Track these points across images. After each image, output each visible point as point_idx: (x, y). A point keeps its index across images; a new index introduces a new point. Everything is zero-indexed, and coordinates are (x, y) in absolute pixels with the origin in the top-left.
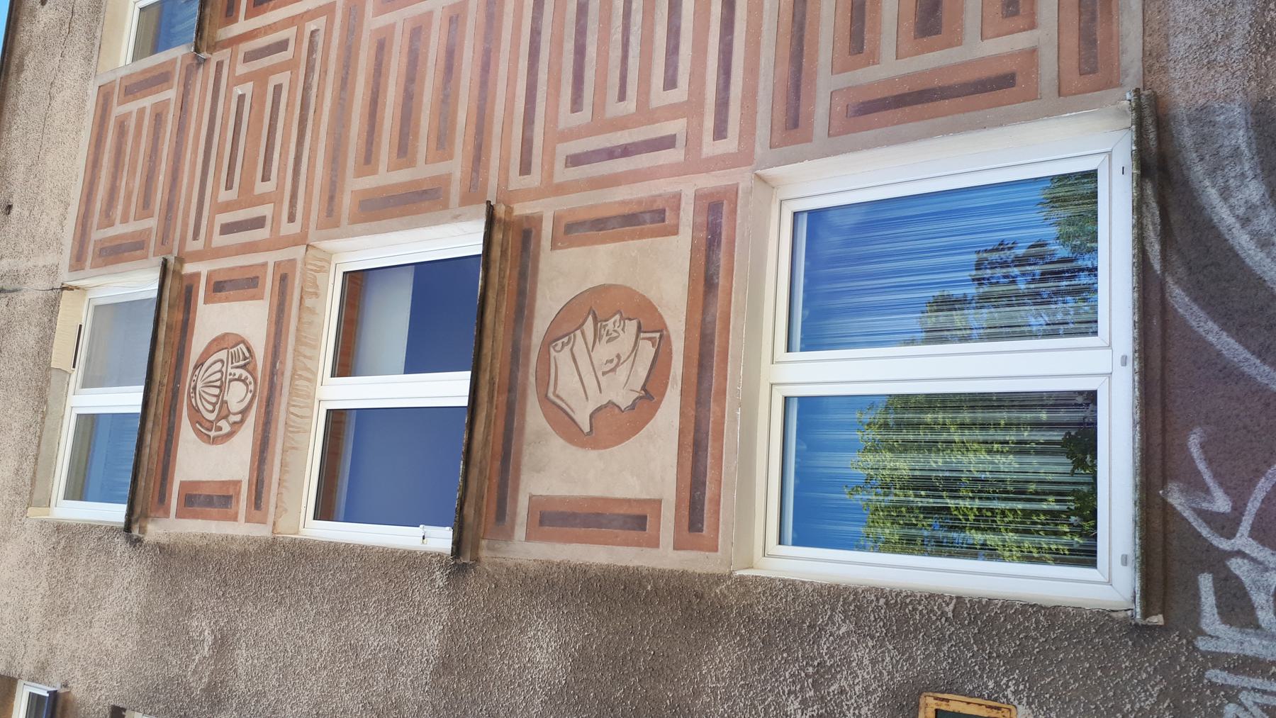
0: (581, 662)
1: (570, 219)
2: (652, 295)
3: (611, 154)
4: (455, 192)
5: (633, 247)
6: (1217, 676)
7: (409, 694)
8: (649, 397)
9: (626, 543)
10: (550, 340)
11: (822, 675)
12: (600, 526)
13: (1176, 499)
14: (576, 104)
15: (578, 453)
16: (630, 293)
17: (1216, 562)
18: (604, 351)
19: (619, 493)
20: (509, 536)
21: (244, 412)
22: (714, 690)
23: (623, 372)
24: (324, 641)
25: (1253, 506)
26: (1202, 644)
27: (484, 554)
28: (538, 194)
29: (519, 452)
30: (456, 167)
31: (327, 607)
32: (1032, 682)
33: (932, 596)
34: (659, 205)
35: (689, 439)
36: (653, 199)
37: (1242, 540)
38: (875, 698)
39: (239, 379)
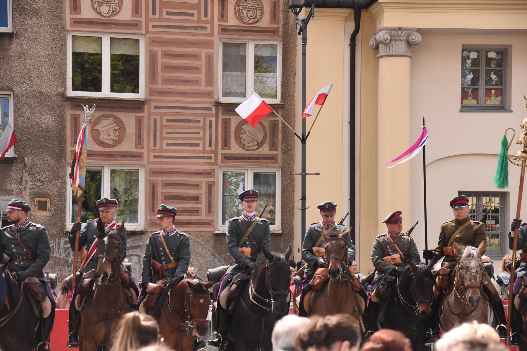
0: (47, 131)
1: (142, 121)
2: (123, 143)
3: (155, 131)
4: (153, 86)
5: (134, 138)
6: (57, 240)
7: (34, 83)
8: (101, 143)
9: (71, 139)
10: (115, 117)
12: (74, 133)
14: (168, 121)
16: (123, 138)
18: (111, 132)
20: (72, 109)
21: (100, 13)
22: (45, 160)
23: (107, 137)
24: (42, 53)
26: (61, 238)
27: (67, 103)
28: (149, 111)
30: (159, 86)
31: (51, 53)
32: (53, 216)
33: (66, 200)
34: (142, 143)
35: (92, 153)
36: (143, 142)
38: (48, 191)
39: (109, 10)
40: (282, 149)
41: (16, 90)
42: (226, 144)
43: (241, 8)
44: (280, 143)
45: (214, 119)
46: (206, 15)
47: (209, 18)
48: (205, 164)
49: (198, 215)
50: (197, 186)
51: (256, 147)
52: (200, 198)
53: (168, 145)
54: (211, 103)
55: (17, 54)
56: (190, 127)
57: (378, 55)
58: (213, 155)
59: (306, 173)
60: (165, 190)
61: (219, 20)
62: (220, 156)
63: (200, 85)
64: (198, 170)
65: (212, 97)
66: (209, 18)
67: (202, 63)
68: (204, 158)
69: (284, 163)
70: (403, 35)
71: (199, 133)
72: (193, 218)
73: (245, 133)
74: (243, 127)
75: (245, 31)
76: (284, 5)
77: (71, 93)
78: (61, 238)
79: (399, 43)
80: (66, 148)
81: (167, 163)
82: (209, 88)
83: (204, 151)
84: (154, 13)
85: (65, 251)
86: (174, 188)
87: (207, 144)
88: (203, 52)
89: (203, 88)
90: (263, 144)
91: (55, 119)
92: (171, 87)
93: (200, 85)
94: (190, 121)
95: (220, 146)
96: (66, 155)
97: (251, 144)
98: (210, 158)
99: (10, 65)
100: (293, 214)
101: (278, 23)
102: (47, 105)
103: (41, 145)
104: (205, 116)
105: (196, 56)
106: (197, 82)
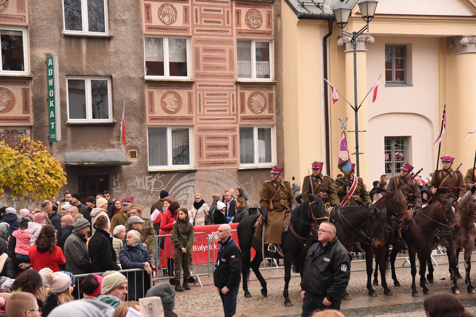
0: (134, 103)
1: (192, 95)
2: (180, 111)
3: (200, 102)
4: (198, 71)
6: (143, 177)
7: (125, 71)
8: (167, 111)
10: (175, 93)
11: (137, 138)
13: (158, 174)
14: (207, 95)
15: (160, 100)
16: (181, 107)
17: (153, 177)
18: (173, 103)
19: (155, 107)
20: (148, 88)
21: (163, 22)
22: (133, 124)
23: (171, 107)
24: (129, 50)
25: (158, 180)
26: (146, 176)
28: (196, 88)
29: (159, 89)
30: (201, 71)
32: (140, 161)
34: (192, 111)
35: (162, 118)
36: (193, 110)
37: (155, 179)
39: (169, 20)
40: (276, 112)
41: (114, 76)
42: (243, 110)
43: (249, 17)
44: (274, 108)
45: (235, 93)
46: (228, 23)
47: (230, 25)
48: (230, 123)
49: (227, 158)
50: (226, 138)
51: (261, 111)
52: (228, 146)
53: (208, 111)
54: (233, 82)
55: (114, 51)
56: (221, 99)
57: (345, 51)
58: (235, 117)
59: (358, 130)
60: (207, 142)
61: (236, 26)
62: (239, 118)
63: (226, 70)
64: (227, 127)
65: (234, 78)
66: (230, 25)
67: (227, 55)
68: (230, 119)
69: (277, 121)
70: (364, 38)
71: (226, 103)
72: (225, 160)
73: (254, 102)
74: (252, 98)
75: (252, 33)
76: (274, 16)
77: (147, 77)
78: (146, 176)
79: (361, 43)
80: (146, 115)
81: (208, 123)
82: (231, 72)
83: (230, 115)
84: (197, 21)
85: (149, 185)
86: (213, 140)
87: (232, 110)
88: (227, 47)
89: (228, 72)
90: (265, 109)
91: (138, 95)
92: (209, 72)
93: (226, 70)
94: (220, 94)
95: (239, 111)
96: (146, 119)
97: (258, 109)
98: (233, 119)
99: (110, 59)
100: (284, 155)
101: (271, 28)
102: (133, 86)
103: (130, 113)
104: (230, 91)
105: (223, 51)
106: (224, 68)
